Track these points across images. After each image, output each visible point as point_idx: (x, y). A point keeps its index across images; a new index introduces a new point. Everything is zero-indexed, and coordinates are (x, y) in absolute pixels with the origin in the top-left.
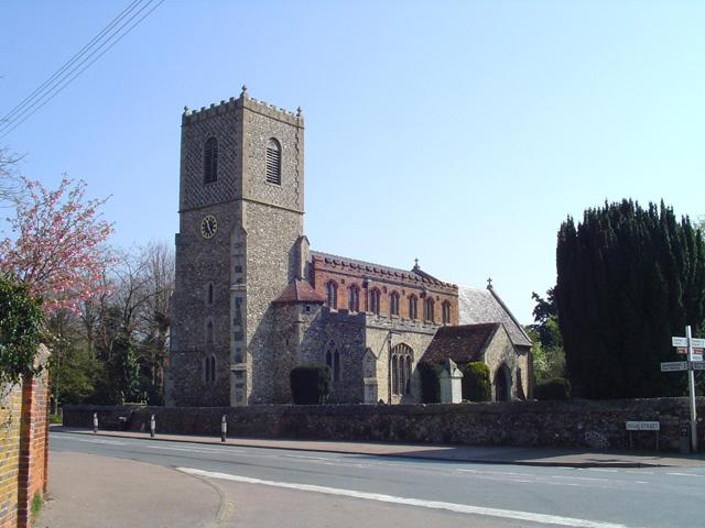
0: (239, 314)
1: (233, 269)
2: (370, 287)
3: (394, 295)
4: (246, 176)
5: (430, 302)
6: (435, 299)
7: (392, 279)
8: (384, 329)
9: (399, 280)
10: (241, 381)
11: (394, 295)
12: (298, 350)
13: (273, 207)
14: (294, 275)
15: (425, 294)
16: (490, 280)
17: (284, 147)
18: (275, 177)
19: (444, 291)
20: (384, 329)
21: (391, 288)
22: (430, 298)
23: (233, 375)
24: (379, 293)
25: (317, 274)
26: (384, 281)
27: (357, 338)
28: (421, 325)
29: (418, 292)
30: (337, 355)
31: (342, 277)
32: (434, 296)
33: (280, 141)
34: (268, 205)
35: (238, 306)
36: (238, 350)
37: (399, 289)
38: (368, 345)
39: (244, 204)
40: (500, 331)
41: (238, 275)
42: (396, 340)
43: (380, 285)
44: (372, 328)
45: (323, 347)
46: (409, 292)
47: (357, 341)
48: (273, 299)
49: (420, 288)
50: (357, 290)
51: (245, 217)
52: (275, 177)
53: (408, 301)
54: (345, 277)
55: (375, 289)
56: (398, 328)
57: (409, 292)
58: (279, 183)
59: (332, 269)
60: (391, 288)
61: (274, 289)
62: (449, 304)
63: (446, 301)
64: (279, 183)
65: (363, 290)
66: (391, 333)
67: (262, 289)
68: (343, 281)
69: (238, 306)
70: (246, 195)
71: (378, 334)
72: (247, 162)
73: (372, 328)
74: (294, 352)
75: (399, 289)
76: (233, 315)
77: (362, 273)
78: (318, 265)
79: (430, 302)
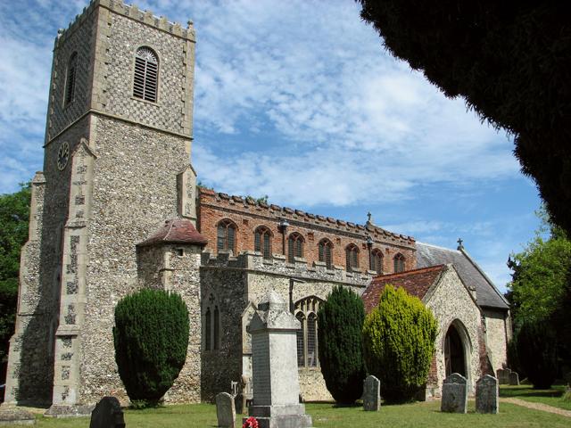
1: (72, 201)
2: (289, 232)
3: (325, 245)
4: (98, 86)
5: (376, 254)
6: (384, 252)
7: (323, 225)
8: (282, 276)
9: (334, 227)
10: (69, 350)
11: (325, 245)
13: (143, 127)
15: (370, 245)
16: (460, 242)
17: (165, 59)
18: (146, 85)
19: (394, 243)
20: (282, 276)
21: (319, 235)
22: (376, 250)
24: (301, 239)
25: (205, 211)
26: (310, 226)
27: (239, 288)
28: (344, 273)
29: (359, 243)
30: (216, 312)
32: (383, 248)
33: (158, 52)
34: (133, 124)
35: (73, 248)
36: (71, 307)
39: (94, 119)
40: (450, 276)
41: (80, 208)
43: (303, 231)
44: (258, 273)
46: (346, 241)
47: (238, 293)
50: (269, 234)
51: (93, 135)
52: (146, 85)
53: (344, 252)
54: (250, 218)
55: (296, 234)
56: (304, 275)
57: (346, 241)
59: (228, 207)
60: (319, 235)
61: (140, 229)
62: (403, 259)
63: (399, 255)
65: (277, 235)
66: (292, 282)
68: (245, 222)
70: (96, 105)
72: (100, 69)
73: (258, 273)
75: (332, 237)
76: (66, 260)
77: (276, 215)
79: (376, 254)
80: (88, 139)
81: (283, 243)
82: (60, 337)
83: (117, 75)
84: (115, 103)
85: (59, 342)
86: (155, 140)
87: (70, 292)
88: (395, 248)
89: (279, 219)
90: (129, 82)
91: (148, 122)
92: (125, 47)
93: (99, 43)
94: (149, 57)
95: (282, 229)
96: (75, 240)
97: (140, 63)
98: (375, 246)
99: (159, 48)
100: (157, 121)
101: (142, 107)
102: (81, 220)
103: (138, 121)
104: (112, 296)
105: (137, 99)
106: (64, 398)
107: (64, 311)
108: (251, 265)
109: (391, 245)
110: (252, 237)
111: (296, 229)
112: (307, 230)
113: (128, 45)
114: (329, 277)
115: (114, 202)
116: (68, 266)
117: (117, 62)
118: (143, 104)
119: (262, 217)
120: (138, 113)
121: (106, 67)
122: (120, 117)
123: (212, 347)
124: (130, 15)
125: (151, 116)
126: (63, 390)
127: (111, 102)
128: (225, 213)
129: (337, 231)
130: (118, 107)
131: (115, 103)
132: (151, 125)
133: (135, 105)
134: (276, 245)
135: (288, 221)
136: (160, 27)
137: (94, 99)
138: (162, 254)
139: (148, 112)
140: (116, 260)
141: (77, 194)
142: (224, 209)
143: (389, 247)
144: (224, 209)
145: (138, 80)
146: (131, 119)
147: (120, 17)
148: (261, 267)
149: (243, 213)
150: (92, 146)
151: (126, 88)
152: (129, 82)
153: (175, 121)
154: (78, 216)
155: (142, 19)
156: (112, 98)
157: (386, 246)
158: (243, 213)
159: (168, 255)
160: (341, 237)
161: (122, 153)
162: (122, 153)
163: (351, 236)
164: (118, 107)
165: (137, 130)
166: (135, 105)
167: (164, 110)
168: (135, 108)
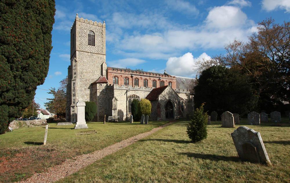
0: (74, 88)
1: (73, 74)
2: (134, 77)
9: (148, 75)
10: (74, 110)
12: (97, 98)
14: (102, 74)
17: (96, 34)
23: (71, 108)
25: (109, 74)
26: (141, 75)
27: (113, 94)
29: (157, 79)
31: (121, 74)
33: (94, 32)
35: (74, 85)
36: (74, 100)
37: (148, 78)
38: (115, 95)
41: (75, 75)
42: (130, 93)
45: (107, 97)
46: (152, 79)
48: (91, 83)
49: (158, 77)
51: (77, 56)
54: (122, 75)
58: (94, 46)
62: (171, 83)
64: (94, 46)
65: (130, 79)
67: (86, 80)
68: (121, 76)
69: (74, 85)
71: (120, 92)
74: (96, 99)
75: (148, 78)
76: (72, 88)
78: (109, 71)
80: (76, 58)
81: (132, 81)
82: (72, 107)
83: (83, 40)
84: (83, 47)
85: (71, 108)
86: (95, 56)
87: (74, 96)
88: (169, 80)
89: (131, 74)
90: (87, 41)
91: (93, 52)
92: (85, 32)
93: (77, 32)
94: (92, 34)
95: (132, 77)
96: (74, 83)
97: (89, 35)
98: (162, 79)
99: (95, 30)
100: (95, 51)
101: (91, 48)
102: (75, 78)
103: (90, 52)
104: (85, 96)
105: (89, 45)
106: (73, 121)
107: (73, 101)
108: (115, 88)
109: (168, 79)
110: (123, 80)
111: (137, 76)
112: (140, 76)
113: (85, 31)
114: (139, 90)
115: (84, 73)
116: (73, 90)
117: (83, 36)
118: (91, 47)
119: (126, 74)
120: (90, 49)
121: (80, 38)
122: (85, 51)
123: (109, 108)
124: (86, 22)
125: (94, 50)
126: (73, 119)
127: (82, 47)
128: (115, 74)
129: (149, 76)
130: (84, 49)
131: (83, 47)
132: (94, 52)
133: (89, 47)
134: (130, 81)
135: (134, 75)
136: (95, 24)
137: (77, 47)
138: (96, 85)
139: (93, 49)
140: (86, 88)
141: (74, 72)
142: (115, 73)
143: (167, 80)
144: (115, 73)
145: (89, 40)
146: (88, 51)
147: (83, 23)
148: (118, 88)
149: (120, 73)
150: (77, 60)
151: (86, 43)
152: (87, 41)
153: (101, 50)
154: (75, 77)
155: (89, 23)
156: (82, 46)
157: (166, 79)
158: (120, 73)
159: (98, 85)
160: (151, 78)
161: (86, 61)
162: (86, 61)
163: (154, 77)
164: (84, 49)
165: (89, 54)
166: (89, 47)
167: (97, 48)
168: (89, 48)
